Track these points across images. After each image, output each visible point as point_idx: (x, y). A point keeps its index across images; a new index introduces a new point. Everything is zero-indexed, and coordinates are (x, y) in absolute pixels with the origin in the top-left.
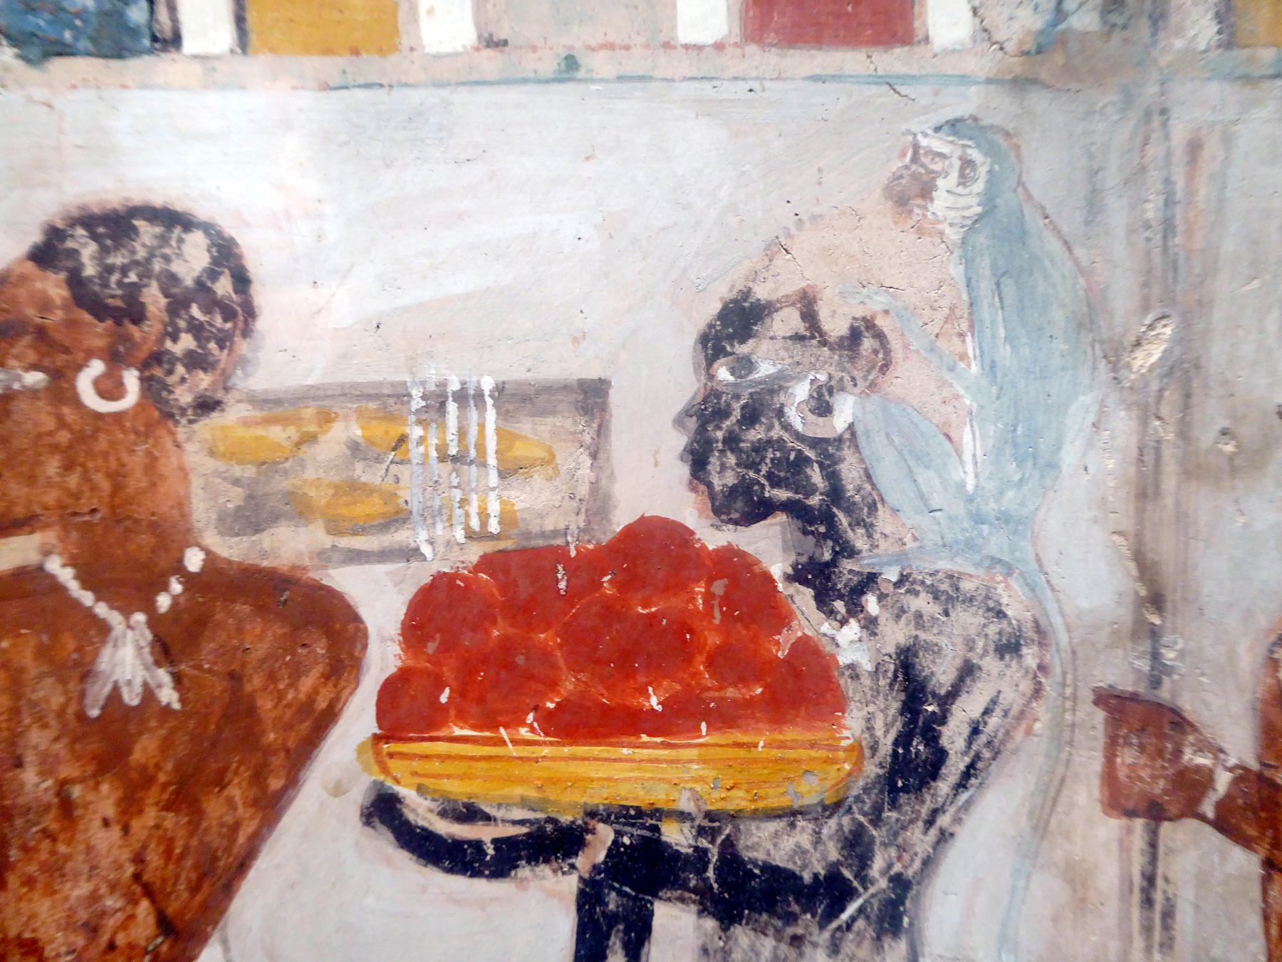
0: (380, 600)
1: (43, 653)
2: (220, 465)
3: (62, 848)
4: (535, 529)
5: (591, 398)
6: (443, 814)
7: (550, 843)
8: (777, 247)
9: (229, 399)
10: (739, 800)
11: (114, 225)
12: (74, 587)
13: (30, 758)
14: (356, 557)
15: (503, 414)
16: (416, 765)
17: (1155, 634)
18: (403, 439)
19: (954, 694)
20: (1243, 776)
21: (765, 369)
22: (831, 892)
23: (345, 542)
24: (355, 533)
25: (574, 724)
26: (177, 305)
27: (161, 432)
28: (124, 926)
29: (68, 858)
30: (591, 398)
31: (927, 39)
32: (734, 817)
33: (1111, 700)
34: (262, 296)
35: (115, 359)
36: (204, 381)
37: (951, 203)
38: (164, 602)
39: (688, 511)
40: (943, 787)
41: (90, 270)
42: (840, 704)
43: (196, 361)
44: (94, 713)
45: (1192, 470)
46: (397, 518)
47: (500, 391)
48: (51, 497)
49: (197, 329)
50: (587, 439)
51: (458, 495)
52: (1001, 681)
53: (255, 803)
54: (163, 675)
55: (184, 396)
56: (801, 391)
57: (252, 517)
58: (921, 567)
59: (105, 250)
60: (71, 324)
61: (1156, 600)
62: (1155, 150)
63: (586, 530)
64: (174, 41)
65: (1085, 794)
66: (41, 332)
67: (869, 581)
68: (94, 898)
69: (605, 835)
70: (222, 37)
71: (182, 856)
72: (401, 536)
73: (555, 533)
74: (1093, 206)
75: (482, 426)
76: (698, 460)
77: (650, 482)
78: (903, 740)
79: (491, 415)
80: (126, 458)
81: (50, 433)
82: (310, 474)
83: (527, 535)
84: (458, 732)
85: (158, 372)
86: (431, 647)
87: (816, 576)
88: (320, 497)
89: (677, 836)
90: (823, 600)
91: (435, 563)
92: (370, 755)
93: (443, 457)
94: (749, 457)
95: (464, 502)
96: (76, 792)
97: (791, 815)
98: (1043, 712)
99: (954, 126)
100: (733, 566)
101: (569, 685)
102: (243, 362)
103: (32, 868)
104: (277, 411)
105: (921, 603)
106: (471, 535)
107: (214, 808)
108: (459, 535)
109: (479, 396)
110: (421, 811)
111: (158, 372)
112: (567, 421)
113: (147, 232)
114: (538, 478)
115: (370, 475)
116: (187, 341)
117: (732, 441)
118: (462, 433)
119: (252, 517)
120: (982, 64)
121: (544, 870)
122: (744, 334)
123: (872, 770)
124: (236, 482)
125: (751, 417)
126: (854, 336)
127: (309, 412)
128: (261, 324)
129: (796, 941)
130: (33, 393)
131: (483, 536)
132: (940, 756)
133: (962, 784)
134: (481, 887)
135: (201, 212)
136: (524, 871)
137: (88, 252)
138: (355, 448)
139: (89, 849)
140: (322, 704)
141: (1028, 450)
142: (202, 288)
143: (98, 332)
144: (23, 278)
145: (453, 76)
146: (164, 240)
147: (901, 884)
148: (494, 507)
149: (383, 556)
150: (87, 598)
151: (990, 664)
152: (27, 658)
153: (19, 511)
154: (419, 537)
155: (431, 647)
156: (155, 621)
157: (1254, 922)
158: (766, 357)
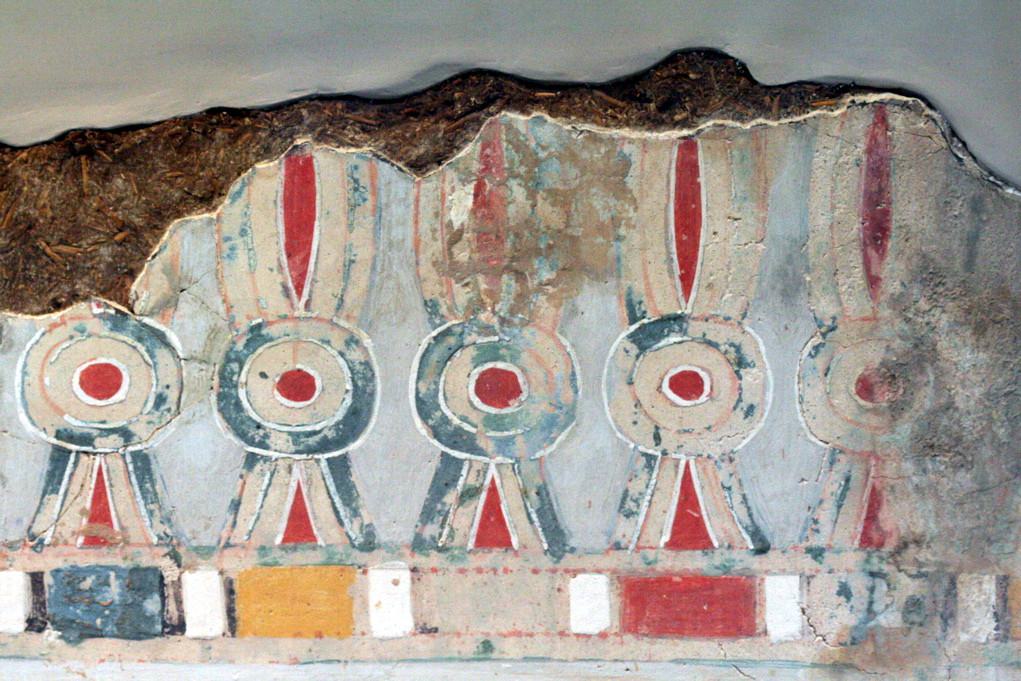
31: (765, 632)
64: (180, 627)
70: (218, 623)
120: (806, 653)
145: (392, 654)
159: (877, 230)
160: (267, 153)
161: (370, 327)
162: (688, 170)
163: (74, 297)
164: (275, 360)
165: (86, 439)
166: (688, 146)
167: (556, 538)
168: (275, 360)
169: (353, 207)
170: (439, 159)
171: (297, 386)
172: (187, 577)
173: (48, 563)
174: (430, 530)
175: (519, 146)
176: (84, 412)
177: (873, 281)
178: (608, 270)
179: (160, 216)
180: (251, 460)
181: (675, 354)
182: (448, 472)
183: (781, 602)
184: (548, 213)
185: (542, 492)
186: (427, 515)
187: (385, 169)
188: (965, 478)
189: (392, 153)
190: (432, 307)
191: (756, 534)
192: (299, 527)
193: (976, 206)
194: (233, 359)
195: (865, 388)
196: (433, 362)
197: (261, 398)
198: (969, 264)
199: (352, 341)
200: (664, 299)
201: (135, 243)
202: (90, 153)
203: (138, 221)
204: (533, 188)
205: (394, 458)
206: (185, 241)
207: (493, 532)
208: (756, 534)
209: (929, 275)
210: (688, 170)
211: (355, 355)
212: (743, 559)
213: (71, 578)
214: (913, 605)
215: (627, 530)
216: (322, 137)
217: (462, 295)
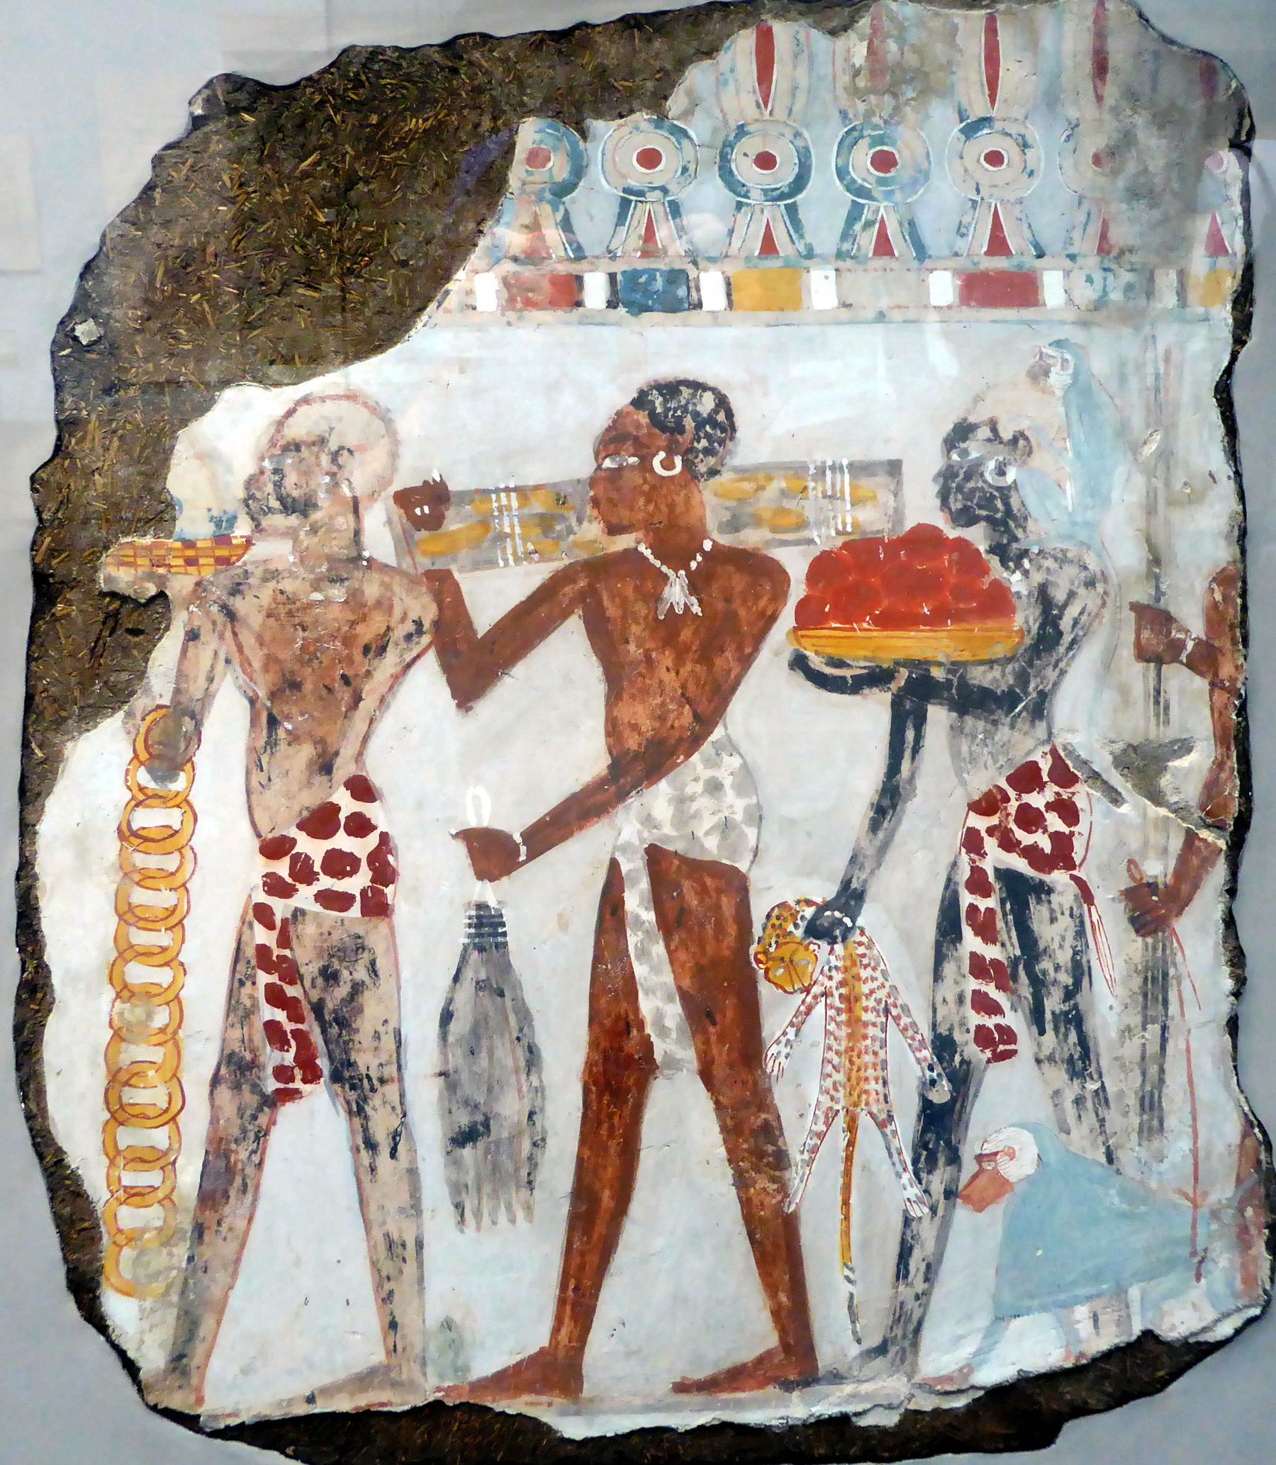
0: (796, 563)
1: (637, 589)
2: (720, 501)
3: (648, 681)
4: (868, 530)
5: (894, 468)
6: (827, 664)
7: (877, 678)
8: (978, 399)
9: (723, 470)
10: (966, 656)
11: (670, 389)
12: (651, 558)
13: (632, 639)
14: (785, 543)
15: (852, 476)
16: (815, 641)
17: (1157, 578)
18: (805, 488)
19: (1065, 605)
20: (1199, 642)
21: (974, 455)
22: (1009, 700)
23: (778, 536)
24: (784, 532)
25: (887, 621)
26: (700, 425)
27: (692, 485)
28: (678, 718)
29: (650, 686)
30: (894, 468)
31: (1045, 304)
32: (964, 664)
33: (1135, 607)
34: (739, 420)
35: (671, 452)
36: (712, 461)
37: (1058, 379)
38: (693, 565)
39: (940, 521)
40: (1062, 649)
41: (659, 410)
42: (1013, 610)
43: (708, 452)
44: (662, 617)
45: (1170, 503)
46: (803, 525)
47: (851, 465)
48: (641, 516)
49: (708, 436)
50: (892, 487)
51: (831, 514)
52: (1088, 599)
53: (739, 660)
54: (694, 600)
55: (702, 468)
56: (991, 465)
57: (734, 525)
58: (1050, 546)
59: (666, 401)
60: (650, 435)
61: (1156, 561)
62: (1150, 355)
63: (893, 530)
64: (699, 305)
65: (1127, 652)
66: (636, 438)
67: (1025, 553)
68: (663, 704)
69: (904, 673)
71: (704, 685)
72: (805, 534)
73: (878, 532)
74: (1123, 379)
75: (843, 482)
76: (944, 496)
77: (922, 507)
78: (1042, 626)
79: (847, 476)
80: (675, 497)
81: (641, 486)
82: (762, 504)
83: (864, 532)
84: (834, 625)
85: (691, 457)
86: (821, 585)
87: (999, 550)
88: (766, 515)
89: (938, 674)
90: (1004, 563)
91: (821, 545)
92: (792, 638)
93: (825, 496)
94: (967, 494)
95: (835, 518)
96: (654, 655)
97: (991, 663)
98: (1107, 615)
99: (1059, 344)
100: (962, 545)
101: (886, 603)
102: (730, 452)
103: (634, 691)
104: (746, 475)
105: (1049, 563)
106: (838, 533)
107: (719, 662)
108: (833, 533)
109: (841, 468)
110: (816, 662)
111: (691, 457)
112: (882, 479)
113: (686, 392)
114: (869, 506)
115: (790, 504)
116: (704, 443)
117: (959, 489)
118: (833, 485)
119: (734, 525)
120: (1070, 315)
121: (875, 690)
122: (965, 439)
123: (1028, 641)
124: (727, 508)
125: (968, 477)
126: (1014, 441)
127: (761, 476)
128: (738, 435)
129: (995, 723)
130: (632, 467)
131: (844, 533)
132: (1061, 634)
133: (1070, 648)
134: (845, 698)
135: (711, 384)
136: (866, 691)
137: (658, 402)
138: (783, 493)
139: (661, 682)
140: (769, 613)
141: (1095, 493)
142: (711, 420)
143: (663, 439)
144: (628, 413)
145: (824, 320)
146: (694, 396)
147: (1043, 696)
148: (849, 520)
149: (797, 543)
150: (658, 563)
151: (1082, 591)
152: (629, 592)
153: (626, 523)
154: (814, 535)
155: (821, 585)
156: (689, 574)
157: (1207, 712)
158: (974, 449)
159: (1101, 67)
160: (744, 26)
161: (807, 126)
162: (991, 31)
163: (632, 111)
164: (753, 146)
165: (640, 193)
166: (991, 20)
167: (921, 252)
168: (753, 146)
169: (796, 56)
170: (845, 29)
171: (766, 161)
172: (702, 275)
173: (619, 267)
174: (846, 246)
175: (893, 19)
176: (638, 176)
177: (1099, 99)
178: (946, 92)
179: (682, 64)
180: (739, 206)
181: (987, 141)
182: (855, 213)
183: (1053, 286)
184: (912, 60)
185: (912, 223)
186: (845, 236)
187: (814, 32)
188: (1156, 214)
189: (816, 25)
190: (844, 114)
191: (1037, 246)
192: (769, 246)
193: (1156, 55)
194: (728, 146)
195: (1097, 160)
196: (848, 143)
197: (745, 169)
198: (1154, 89)
199: (797, 134)
200: (979, 108)
201: (666, 82)
202: (639, 27)
203: (668, 67)
204: (901, 40)
205: (824, 204)
206: (698, 76)
207: (884, 247)
208: (1037, 246)
209: (1132, 96)
210: (991, 31)
211: (799, 143)
212: (1030, 262)
213: (632, 276)
214: (1129, 288)
215: (961, 245)
216: (776, 16)
217: (861, 107)
